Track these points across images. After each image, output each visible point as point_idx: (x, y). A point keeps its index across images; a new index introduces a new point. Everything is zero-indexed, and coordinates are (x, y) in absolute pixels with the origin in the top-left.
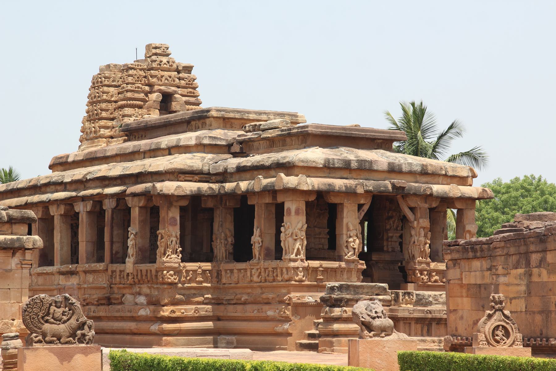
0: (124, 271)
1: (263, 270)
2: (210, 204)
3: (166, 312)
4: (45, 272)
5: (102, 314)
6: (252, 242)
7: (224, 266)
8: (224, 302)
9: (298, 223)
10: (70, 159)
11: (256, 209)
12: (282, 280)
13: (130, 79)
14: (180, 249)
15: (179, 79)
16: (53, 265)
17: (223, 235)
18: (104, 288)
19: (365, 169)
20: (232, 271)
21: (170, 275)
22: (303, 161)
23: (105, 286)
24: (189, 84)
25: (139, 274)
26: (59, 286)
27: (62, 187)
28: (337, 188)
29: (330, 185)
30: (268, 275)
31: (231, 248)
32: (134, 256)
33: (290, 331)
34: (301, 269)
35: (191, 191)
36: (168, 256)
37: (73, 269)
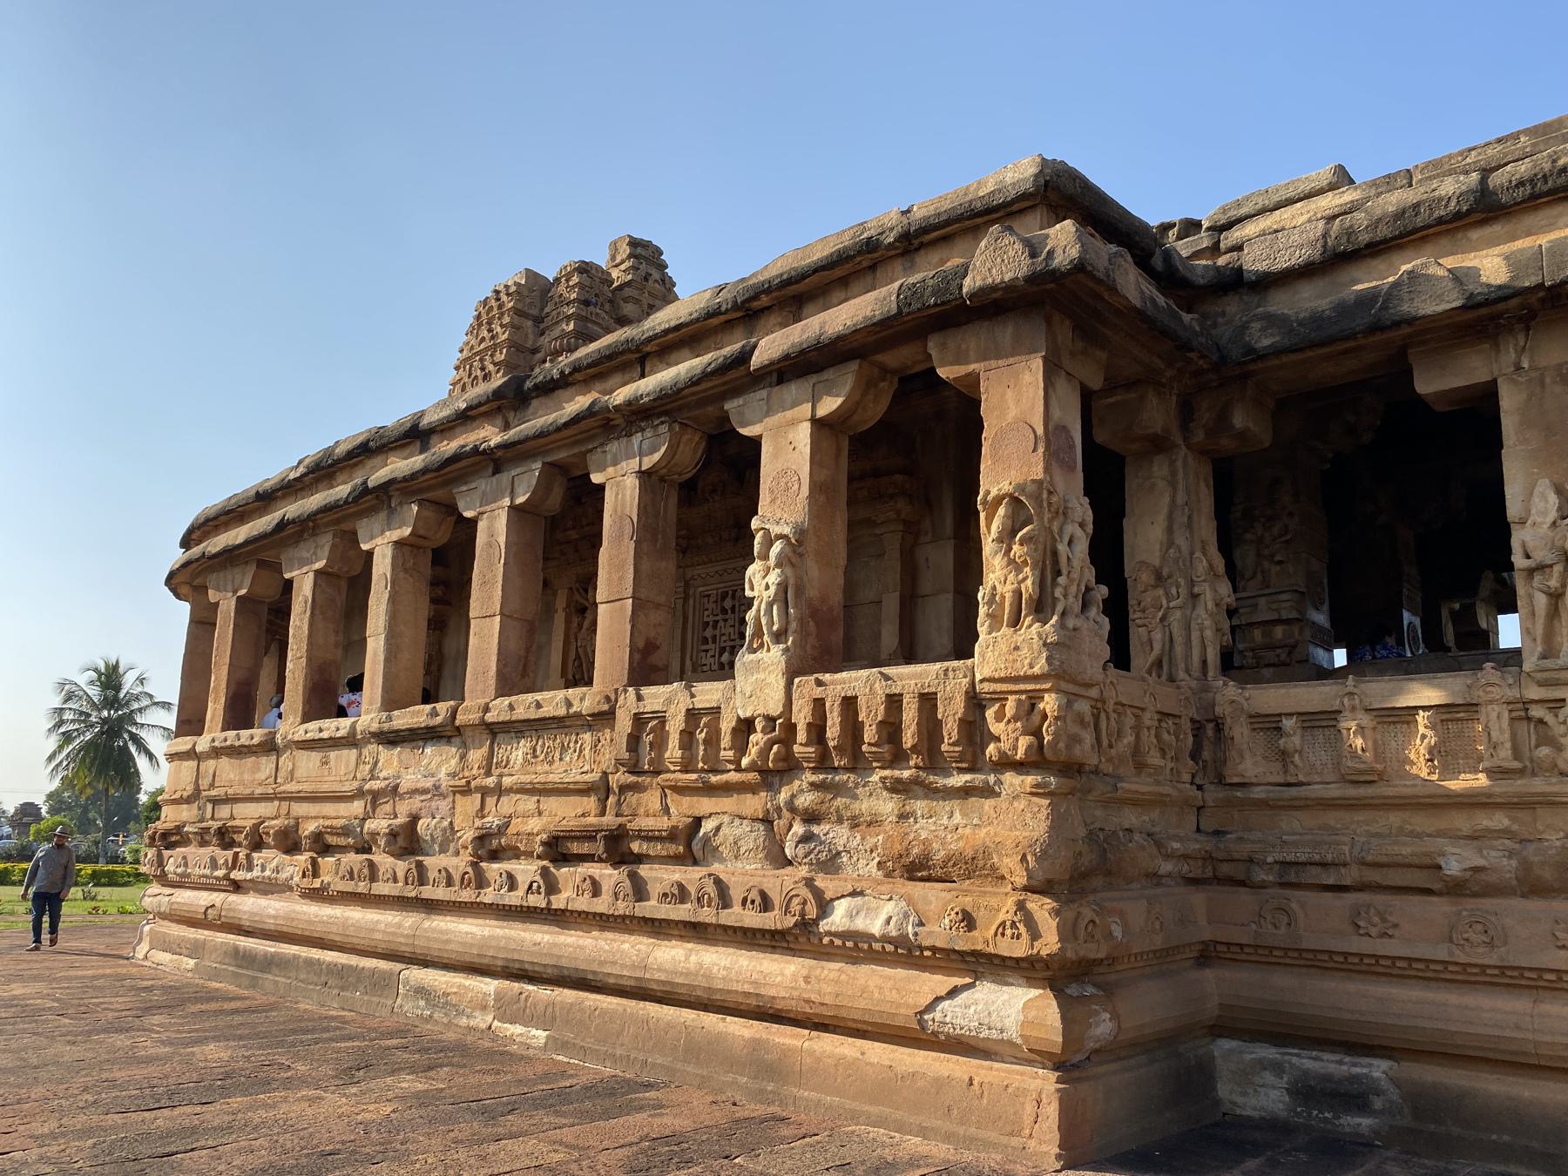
0: (715, 711)
6: (1518, 560)
8: (1261, 876)
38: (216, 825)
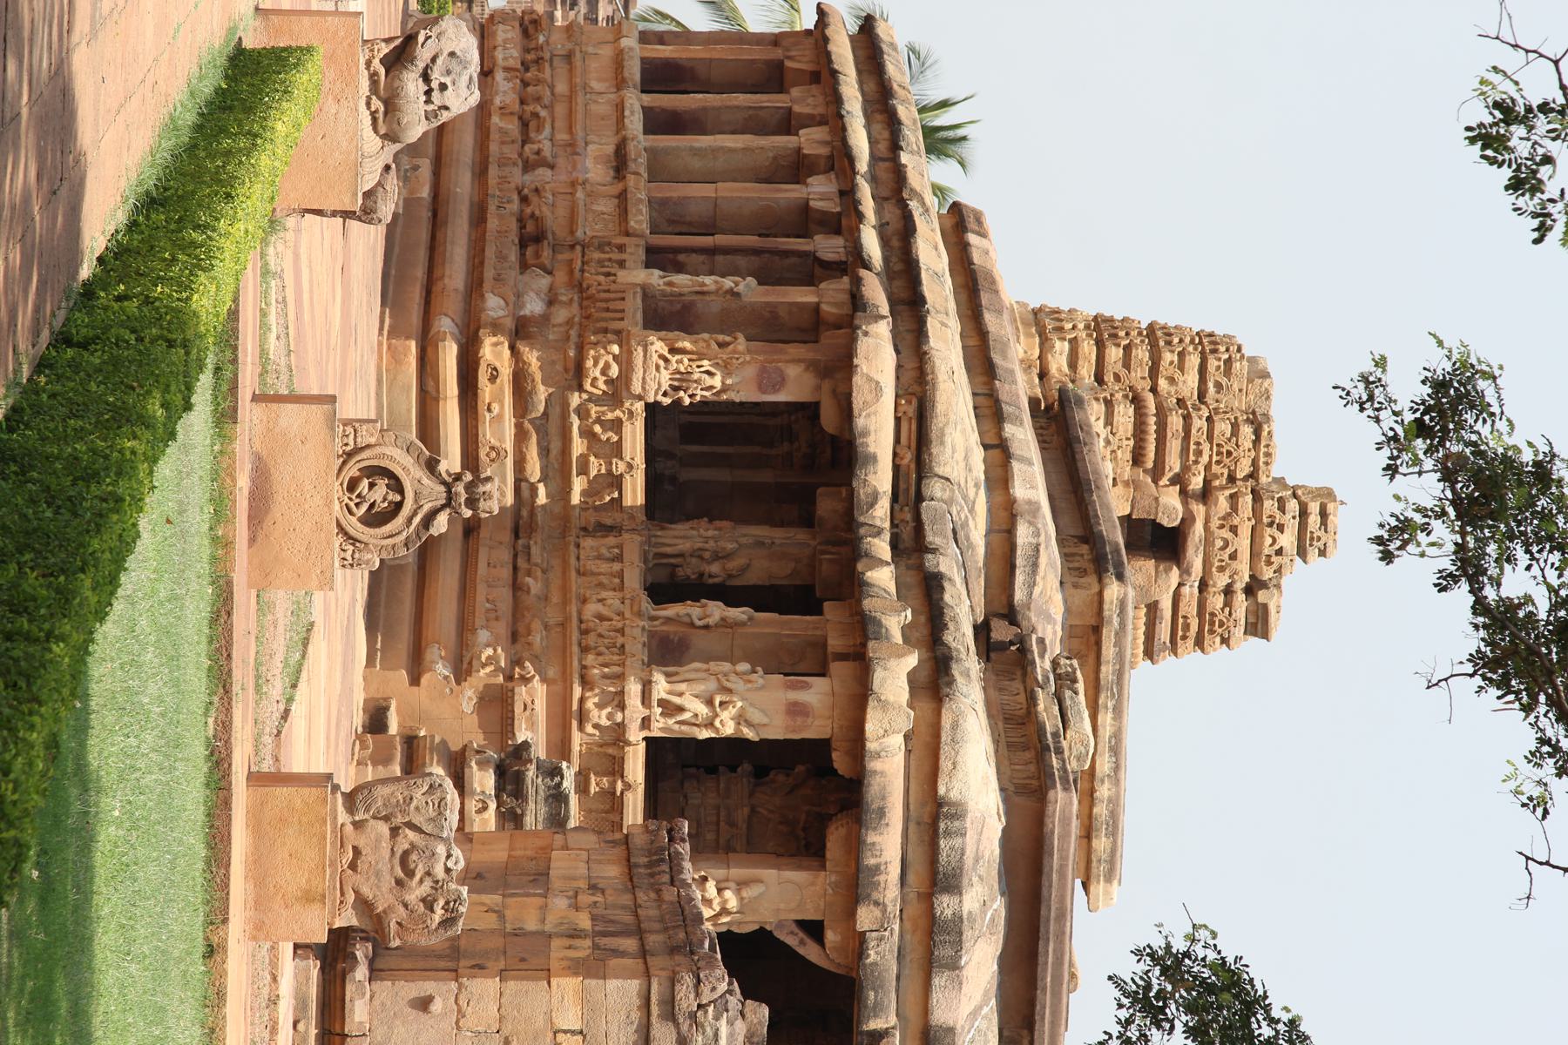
1: (620, 625)
2: (826, 505)
3: (494, 352)
4: (627, 113)
5: (492, 223)
7: (632, 545)
8: (520, 542)
9: (762, 711)
10: (972, 238)
11: (808, 618)
12: (584, 667)
13: (1222, 427)
14: (687, 401)
15: (1228, 591)
16: (645, 132)
17: (730, 546)
18: (572, 232)
19: (934, 944)
20: (619, 558)
21: (607, 366)
22: (955, 726)
23: (579, 234)
24: (1212, 623)
25: (612, 296)
26: (581, 143)
27: (883, 147)
28: (871, 838)
29: (881, 813)
30: (600, 636)
31: (689, 571)
32: (668, 289)
33: (424, 680)
34: (619, 717)
35: (865, 433)
36: (666, 360)
37: (632, 166)
38: (547, 56)
